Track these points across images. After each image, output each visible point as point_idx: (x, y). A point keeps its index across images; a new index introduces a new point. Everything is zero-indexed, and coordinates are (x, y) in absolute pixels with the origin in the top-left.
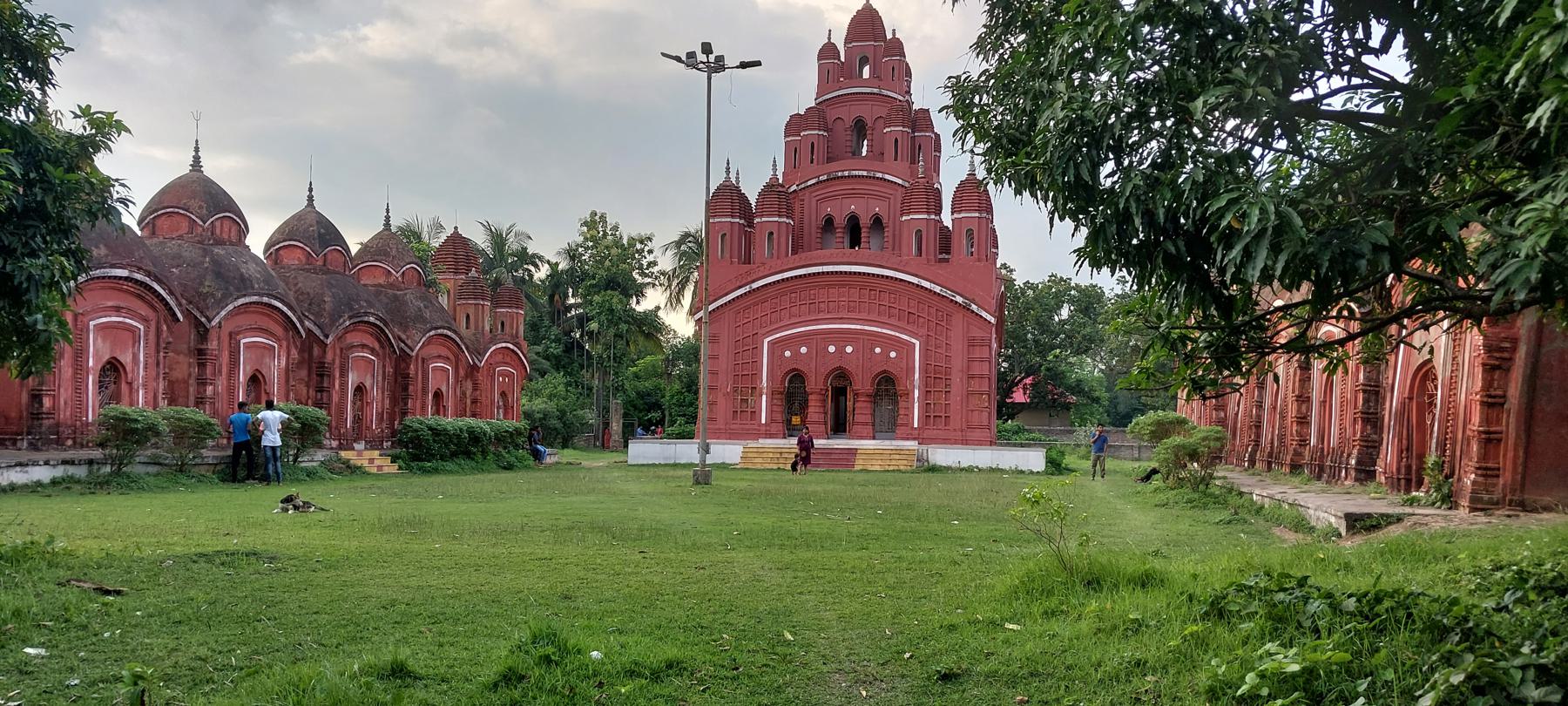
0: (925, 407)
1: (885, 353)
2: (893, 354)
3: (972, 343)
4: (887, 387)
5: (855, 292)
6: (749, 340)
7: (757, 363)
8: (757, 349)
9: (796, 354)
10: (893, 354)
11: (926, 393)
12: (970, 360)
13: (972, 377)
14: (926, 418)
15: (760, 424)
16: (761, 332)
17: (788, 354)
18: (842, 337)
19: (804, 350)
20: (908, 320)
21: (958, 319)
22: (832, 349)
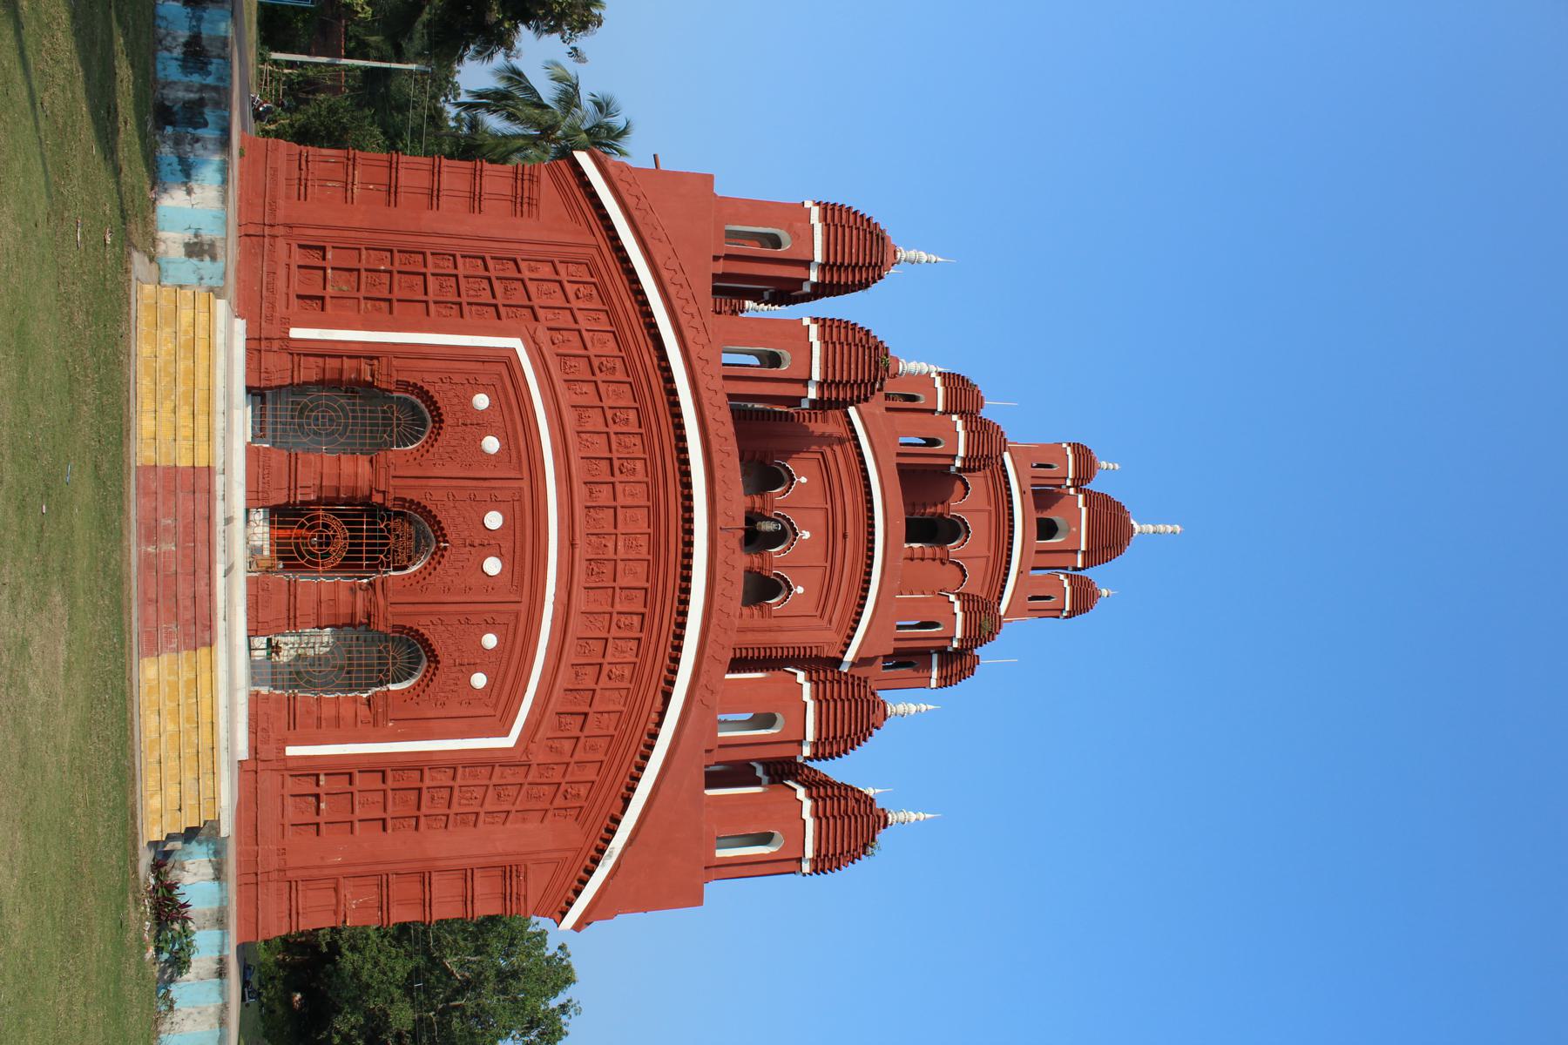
0: (344, 770)
1: (482, 660)
2: (479, 680)
3: (509, 873)
4: (395, 656)
5: (633, 576)
6: (519, 297)
7: (457, 314)
8: (495, 316)
9: (482, 424)
10: (479, 680)
11: (379, 768)
12: (467, 875)
13: (425, 878)
14: (311, 770)
15: (288, 323)
16: (543, 336)
17: (481, 401)
18: (522, 546)
19: (491, 444)
20: (567, 712)
21: (577, 836)
22: (494, 520)
